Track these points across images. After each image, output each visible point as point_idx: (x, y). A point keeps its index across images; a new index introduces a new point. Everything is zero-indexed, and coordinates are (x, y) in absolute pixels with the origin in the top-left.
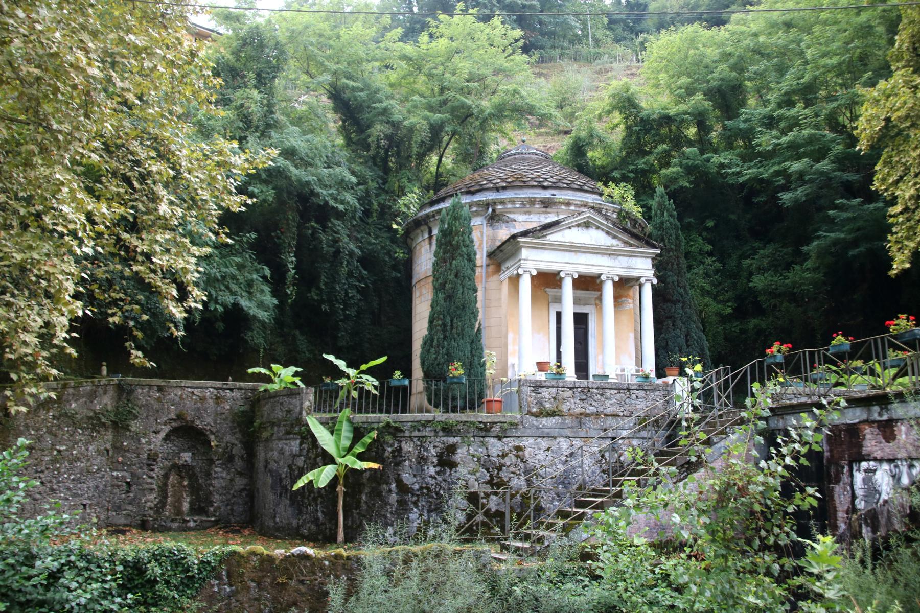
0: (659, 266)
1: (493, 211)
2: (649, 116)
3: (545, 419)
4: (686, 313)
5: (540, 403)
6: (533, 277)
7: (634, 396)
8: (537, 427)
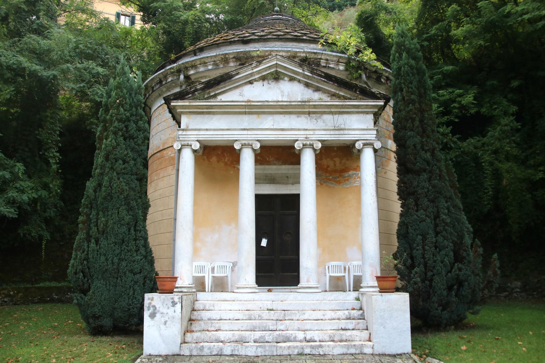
1: (187, 78)
4: (434, 187)
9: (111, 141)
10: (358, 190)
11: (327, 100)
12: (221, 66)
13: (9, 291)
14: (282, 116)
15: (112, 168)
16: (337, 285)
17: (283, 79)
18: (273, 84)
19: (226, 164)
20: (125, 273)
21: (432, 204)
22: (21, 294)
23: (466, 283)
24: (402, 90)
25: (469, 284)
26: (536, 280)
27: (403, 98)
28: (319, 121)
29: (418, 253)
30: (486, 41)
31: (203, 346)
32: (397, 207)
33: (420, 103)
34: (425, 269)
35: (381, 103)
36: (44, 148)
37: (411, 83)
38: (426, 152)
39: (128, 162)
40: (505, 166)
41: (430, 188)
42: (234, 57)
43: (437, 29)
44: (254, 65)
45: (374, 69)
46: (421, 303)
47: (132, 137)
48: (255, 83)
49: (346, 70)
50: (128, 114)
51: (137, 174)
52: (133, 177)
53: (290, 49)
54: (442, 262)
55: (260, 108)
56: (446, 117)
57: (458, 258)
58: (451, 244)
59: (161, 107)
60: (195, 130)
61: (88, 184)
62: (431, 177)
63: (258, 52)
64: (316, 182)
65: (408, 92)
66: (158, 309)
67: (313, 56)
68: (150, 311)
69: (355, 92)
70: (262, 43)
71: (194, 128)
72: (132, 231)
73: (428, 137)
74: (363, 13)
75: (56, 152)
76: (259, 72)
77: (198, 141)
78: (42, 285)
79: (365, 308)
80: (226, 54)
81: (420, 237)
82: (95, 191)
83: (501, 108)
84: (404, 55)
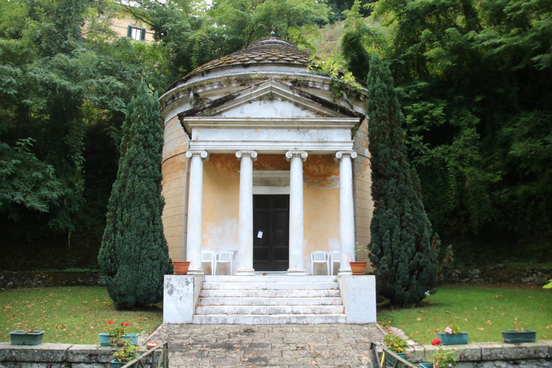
1: (196, 95)
2: (413, 8)
4: (401, 189)
9: (133, 150)
10: (337, 192)
11: (312, 117)
12: (225, 86)
13: (42, 275)
14: (275, 130)
15: (134, 172)
16: (321, 270)
17: (276, 99)
18: (268, 103)
19: (228, 169)
20: (145, 260)
21: (398, 204)
22: (51, 278)
23: (425, 269)
24: (375, 108)
25: (427, 269)
26: (492, 268)
27: (377, 115)
28: (306, 134)
29: (385, 244)
30: (453, 62)
31: (210, 317)
32: (370, 205)
33: (390, 120)
34: (392, 257)
35: (357, 120)
36: (70, 152)
37: (383, 102)
38: (394, 161)
39: (147, 168)
40: (467, 170)
41: (397, 190)
42: (236, 79)
43: (412, 50)
44: (252, 88)
45: (354, 89)
46: (388, 285)
47: (150, 146)
48: (253, 102)
49: (330, 90)
50: (147, 127)
51: (154, 178)
52: (151, 180)
53: (283, 73)
54: (406, 251)
55: (258, 124)
56: (419, 127)
57: (419, 248)
58: (413, 237)
59: (173, 119)
60: (204, 141)
61: (114, 185)
62: (398, 182)
63: (256, 75)
64: (304, 185)
65: (380, 110)
66: (175, 287)
67: (302, 79)
68: (169, 289)
69: (336, 110)
70: (259, 67)
71: (203, 139)
72: (151, 225)
73: (396, 148)
74: (348, 34)
75: (81, 155)
76: (256, 94)
77: (206, 150)
78: (68, 270)
79: (341, 288)
80: (229, 76)
81: (388, 231)
82: (120, 191)
83: (466, 119)
84: (378, 79)
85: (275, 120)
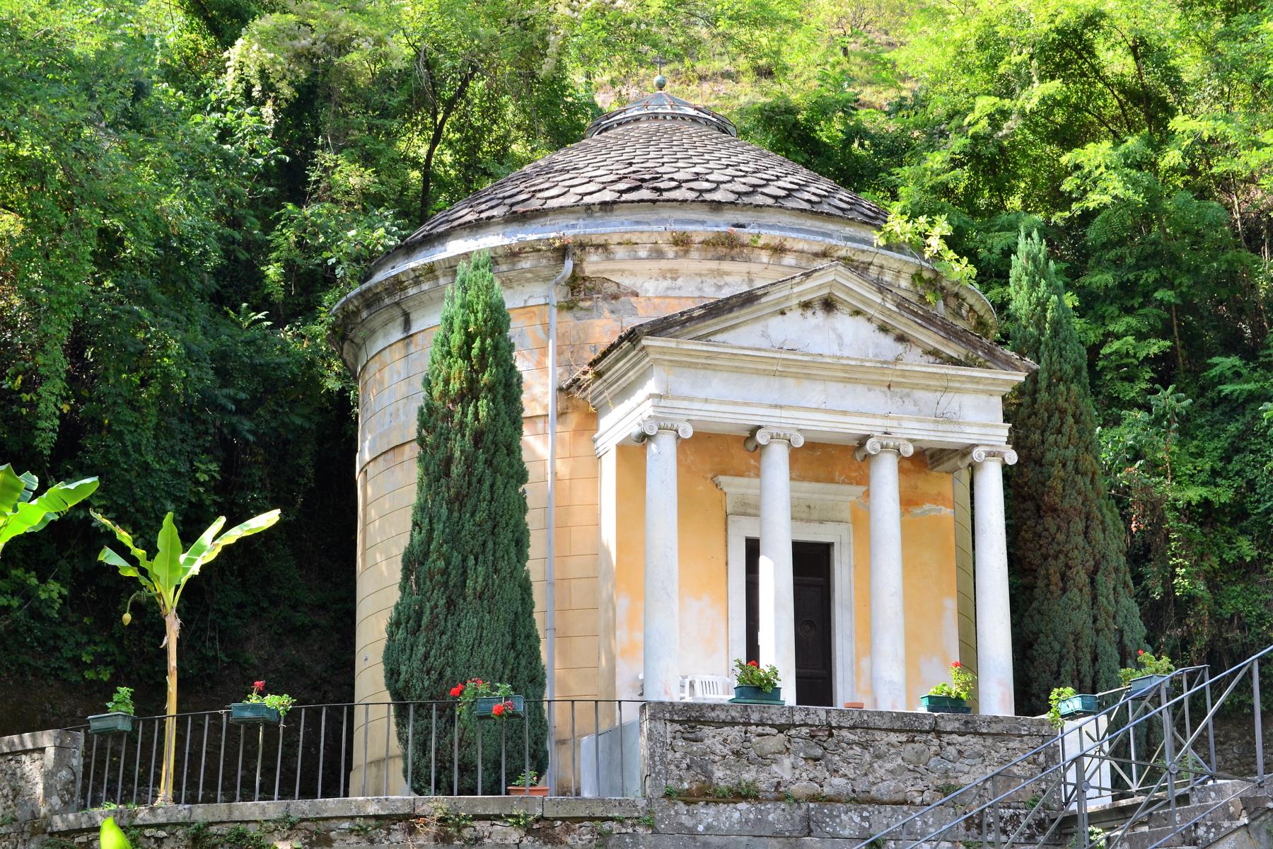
0: (1021, 411)
3: (712, 810)
5: (700, 765)
6: (682, 443)
7: (952, 751)
8: (692, 833)
14: (841, 385)
44: (797, 280)
85: (845, 362)
